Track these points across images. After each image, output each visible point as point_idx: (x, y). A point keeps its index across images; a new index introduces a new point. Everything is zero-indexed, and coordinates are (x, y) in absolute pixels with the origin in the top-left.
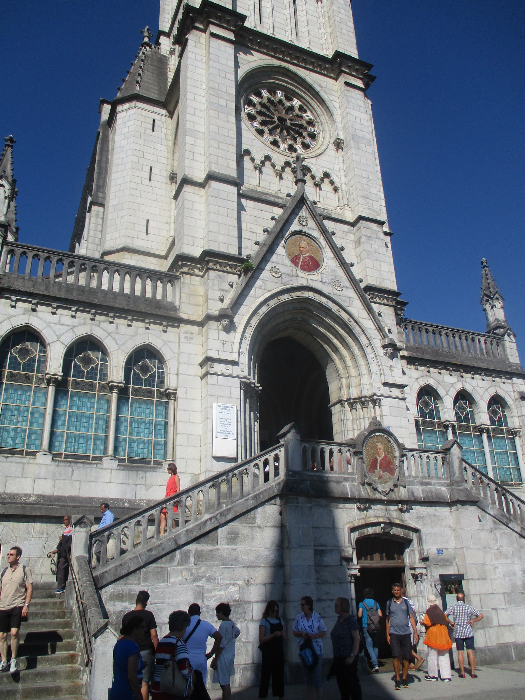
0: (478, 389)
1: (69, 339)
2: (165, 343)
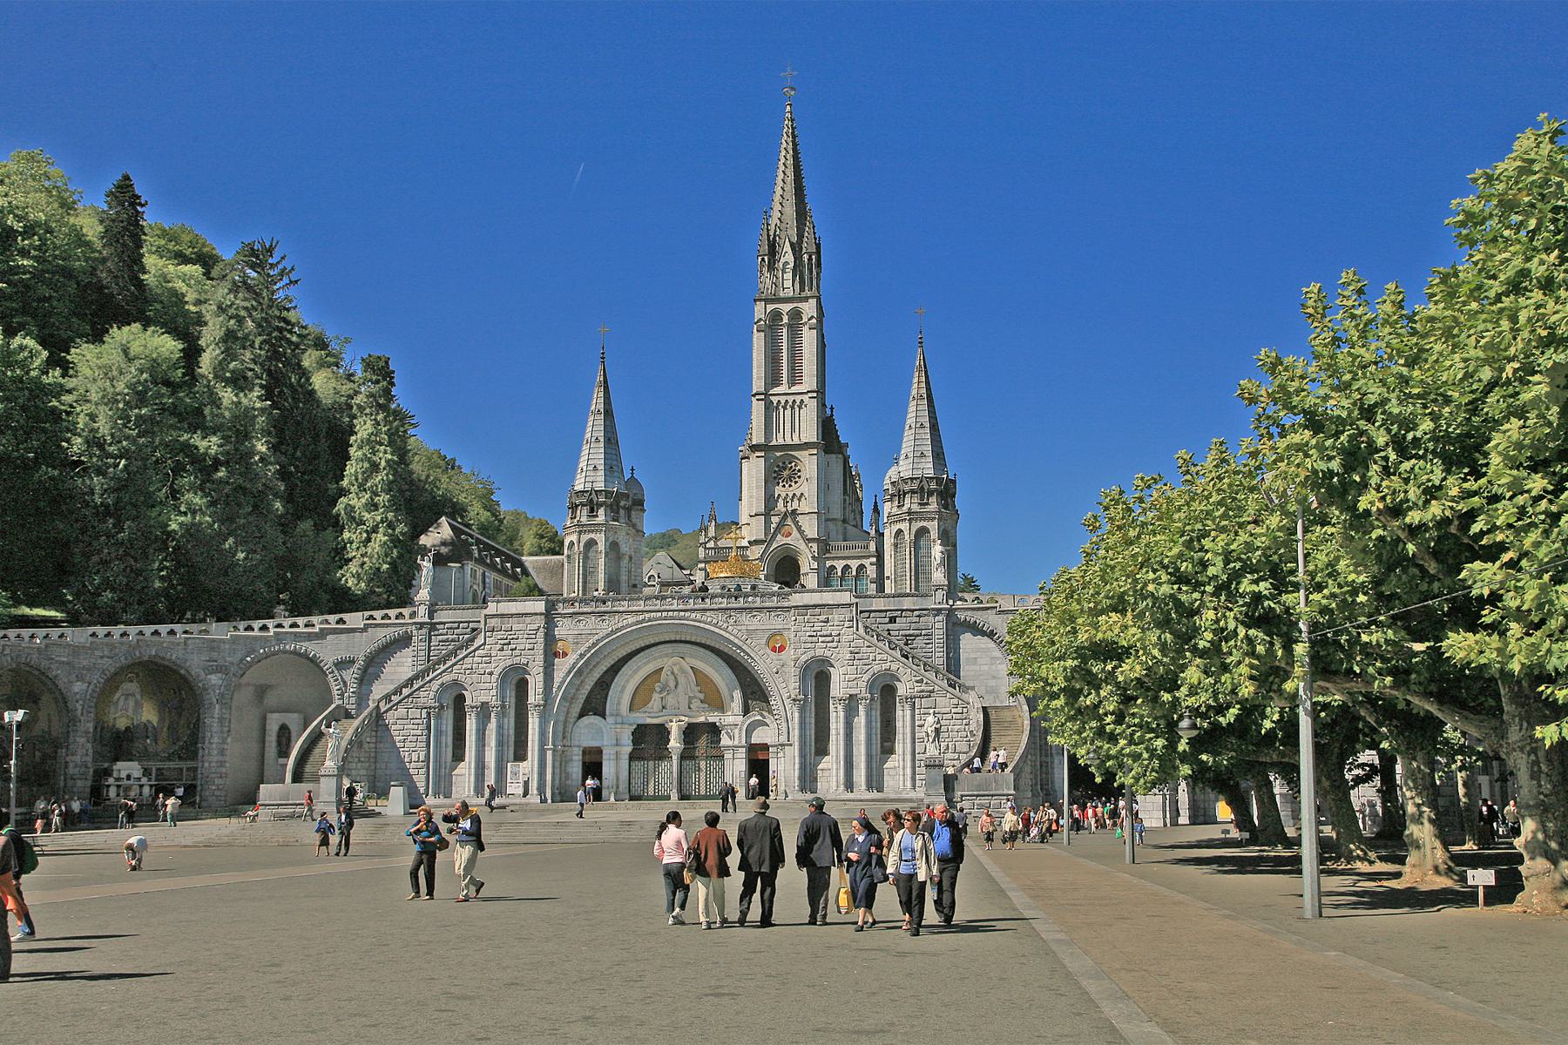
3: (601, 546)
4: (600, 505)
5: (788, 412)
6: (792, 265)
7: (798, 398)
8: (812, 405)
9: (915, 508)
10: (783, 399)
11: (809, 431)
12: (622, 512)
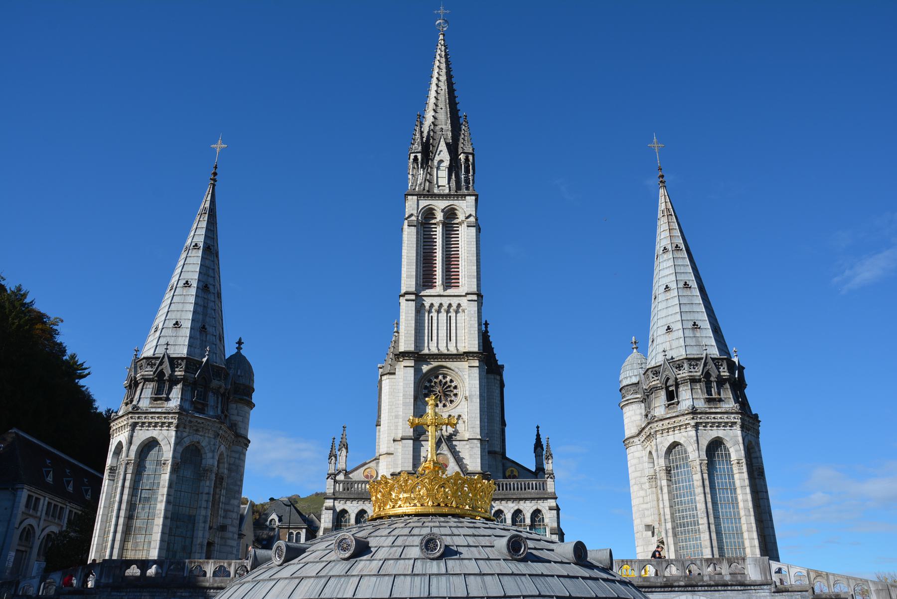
0: (527, 508)
1: (356, 511)
3: (167, 452)
4: (173, 381)
5: (443, 315)
6: (446, 163)
7: (455, 302)
8: (470, 308)
9: (701, 405)
10: (436, 301)
11: (469, 342)
12: (211, 399)
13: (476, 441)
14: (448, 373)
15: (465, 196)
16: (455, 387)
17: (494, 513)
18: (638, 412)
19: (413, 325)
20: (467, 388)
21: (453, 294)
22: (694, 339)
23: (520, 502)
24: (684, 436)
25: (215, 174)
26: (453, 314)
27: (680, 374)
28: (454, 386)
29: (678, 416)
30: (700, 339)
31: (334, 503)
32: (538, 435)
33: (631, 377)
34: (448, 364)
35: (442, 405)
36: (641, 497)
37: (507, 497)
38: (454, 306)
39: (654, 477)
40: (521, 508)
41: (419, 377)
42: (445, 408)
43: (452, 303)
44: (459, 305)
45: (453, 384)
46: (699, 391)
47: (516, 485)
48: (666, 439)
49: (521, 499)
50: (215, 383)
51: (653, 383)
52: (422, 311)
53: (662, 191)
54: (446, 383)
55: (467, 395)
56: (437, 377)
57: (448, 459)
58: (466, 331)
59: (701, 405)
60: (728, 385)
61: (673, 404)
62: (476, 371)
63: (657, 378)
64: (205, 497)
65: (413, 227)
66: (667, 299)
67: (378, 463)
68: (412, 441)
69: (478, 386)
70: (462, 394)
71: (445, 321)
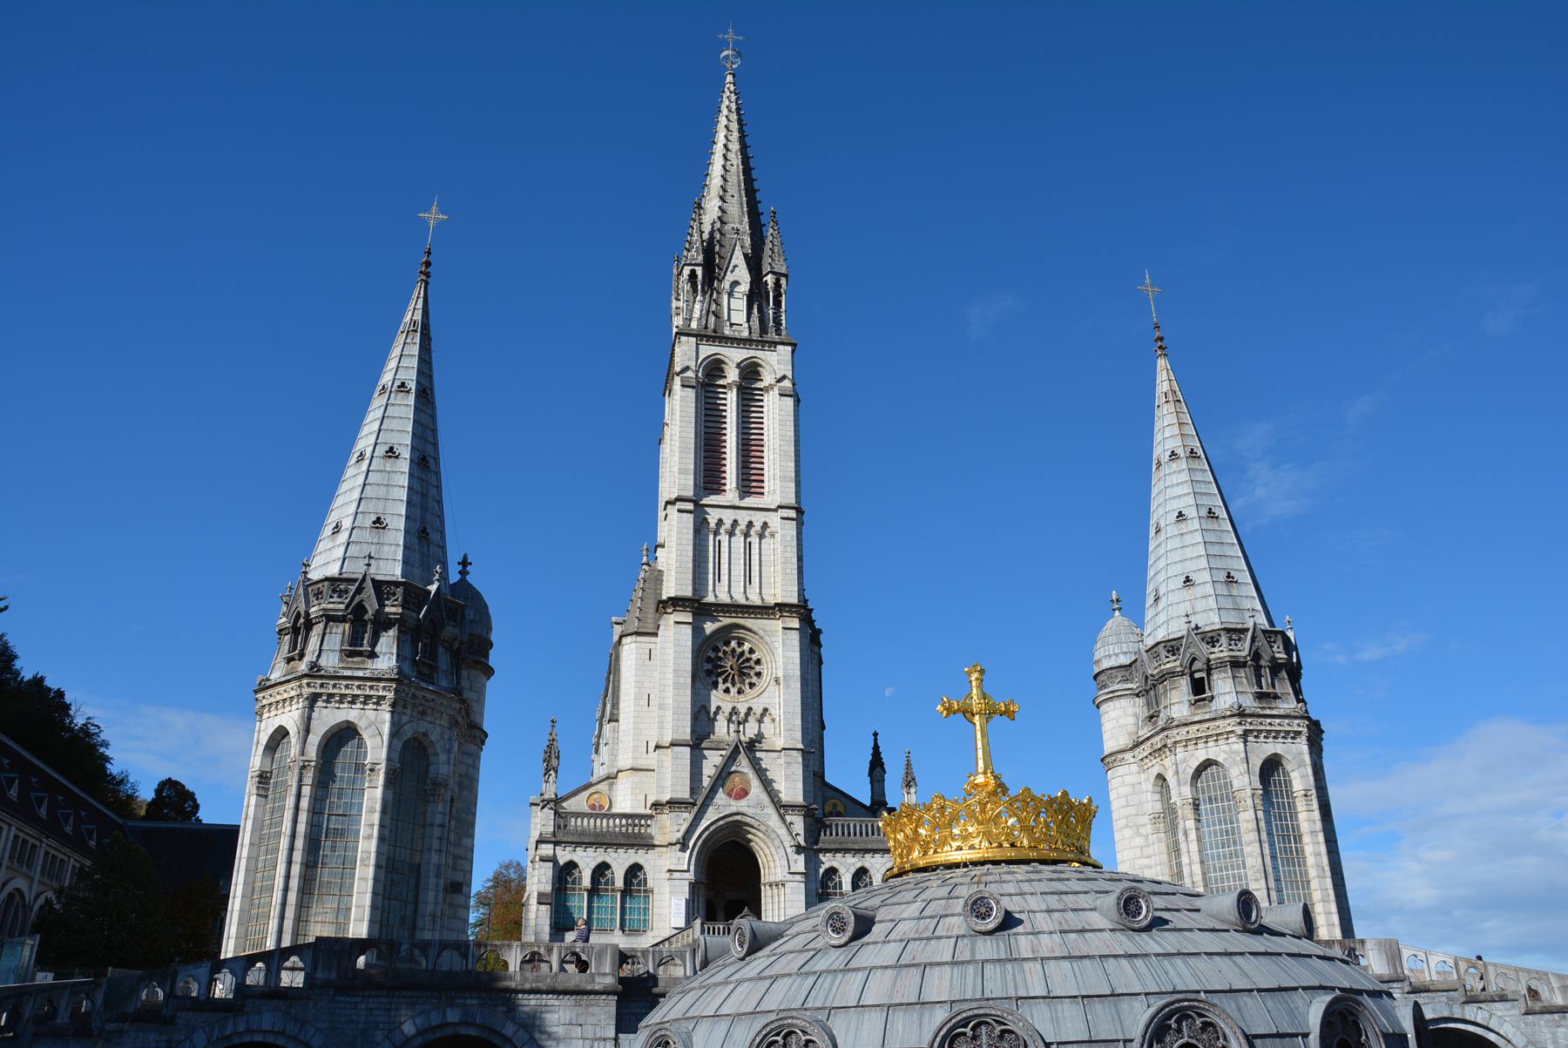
1: (593, 865)
2: (646, 860)
3: (376, 748)
4: (382, 623)
5: (738, 541)
8: (783, 532)
9: (1249, 703)
10: (728, 516)
11: (780, 586)
13: (794, 753)
14: (747, 637)
15: (775, 344)
16: (758, 662)
17: (823, 874)
18: (1130, 711)
19: (691, 554)
20: (780, 663)
21: (756, 506)
22: (1230, 599)
23: (867, 855)
24: (1223, 752)
25: (428, 264)
26: (755, 540)
27: (1214, 653)
28: (755, 659)
29: (1214, 719)
30: (1238, 599)
31: (554, 849)
32: (876, 748)
33: (1117, 655)
34: (748, 623)
35: (736, 690)
36: (1137, 847)
37: (844, 846)
38: (757, 527)
39: (1162, 815)
40: (867, 865)
41: (699, 642)
42: (742, 695)
43: (754, 520)
44: (765, 526)
45: (754, 657)
46: (1244, 680)
47: (858, 828)
48: (1193, 755)
49: (867, 851)
50: (449, 631)
51: (1168, 666)
52: (704, 531)
53: (1162, 363)
54: (742, 653)
55: (780, 675)
56: (727, 643)
57: (748, 782)
58: (779, 568)
59: (1249, 703)
60: (1284, 674)
61: (1204, 699)
62: (795, 636)
63: (1174, 658)
64: (437, 832)
65: (691, 390)
66: (1182, 534)
67: (611, 785)
68: (688, 749)
69: (798, 661)
70: (770, 673)
71: (742, 550)
